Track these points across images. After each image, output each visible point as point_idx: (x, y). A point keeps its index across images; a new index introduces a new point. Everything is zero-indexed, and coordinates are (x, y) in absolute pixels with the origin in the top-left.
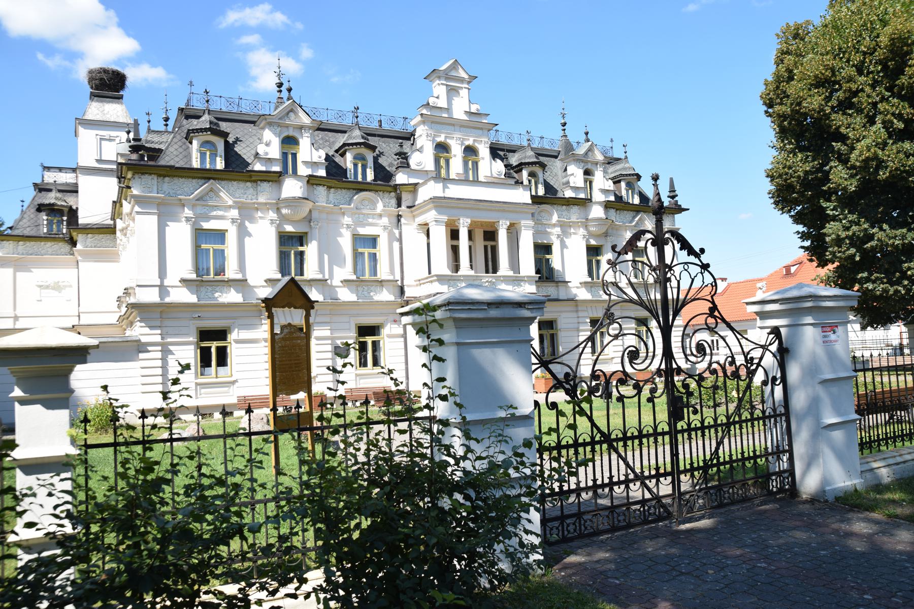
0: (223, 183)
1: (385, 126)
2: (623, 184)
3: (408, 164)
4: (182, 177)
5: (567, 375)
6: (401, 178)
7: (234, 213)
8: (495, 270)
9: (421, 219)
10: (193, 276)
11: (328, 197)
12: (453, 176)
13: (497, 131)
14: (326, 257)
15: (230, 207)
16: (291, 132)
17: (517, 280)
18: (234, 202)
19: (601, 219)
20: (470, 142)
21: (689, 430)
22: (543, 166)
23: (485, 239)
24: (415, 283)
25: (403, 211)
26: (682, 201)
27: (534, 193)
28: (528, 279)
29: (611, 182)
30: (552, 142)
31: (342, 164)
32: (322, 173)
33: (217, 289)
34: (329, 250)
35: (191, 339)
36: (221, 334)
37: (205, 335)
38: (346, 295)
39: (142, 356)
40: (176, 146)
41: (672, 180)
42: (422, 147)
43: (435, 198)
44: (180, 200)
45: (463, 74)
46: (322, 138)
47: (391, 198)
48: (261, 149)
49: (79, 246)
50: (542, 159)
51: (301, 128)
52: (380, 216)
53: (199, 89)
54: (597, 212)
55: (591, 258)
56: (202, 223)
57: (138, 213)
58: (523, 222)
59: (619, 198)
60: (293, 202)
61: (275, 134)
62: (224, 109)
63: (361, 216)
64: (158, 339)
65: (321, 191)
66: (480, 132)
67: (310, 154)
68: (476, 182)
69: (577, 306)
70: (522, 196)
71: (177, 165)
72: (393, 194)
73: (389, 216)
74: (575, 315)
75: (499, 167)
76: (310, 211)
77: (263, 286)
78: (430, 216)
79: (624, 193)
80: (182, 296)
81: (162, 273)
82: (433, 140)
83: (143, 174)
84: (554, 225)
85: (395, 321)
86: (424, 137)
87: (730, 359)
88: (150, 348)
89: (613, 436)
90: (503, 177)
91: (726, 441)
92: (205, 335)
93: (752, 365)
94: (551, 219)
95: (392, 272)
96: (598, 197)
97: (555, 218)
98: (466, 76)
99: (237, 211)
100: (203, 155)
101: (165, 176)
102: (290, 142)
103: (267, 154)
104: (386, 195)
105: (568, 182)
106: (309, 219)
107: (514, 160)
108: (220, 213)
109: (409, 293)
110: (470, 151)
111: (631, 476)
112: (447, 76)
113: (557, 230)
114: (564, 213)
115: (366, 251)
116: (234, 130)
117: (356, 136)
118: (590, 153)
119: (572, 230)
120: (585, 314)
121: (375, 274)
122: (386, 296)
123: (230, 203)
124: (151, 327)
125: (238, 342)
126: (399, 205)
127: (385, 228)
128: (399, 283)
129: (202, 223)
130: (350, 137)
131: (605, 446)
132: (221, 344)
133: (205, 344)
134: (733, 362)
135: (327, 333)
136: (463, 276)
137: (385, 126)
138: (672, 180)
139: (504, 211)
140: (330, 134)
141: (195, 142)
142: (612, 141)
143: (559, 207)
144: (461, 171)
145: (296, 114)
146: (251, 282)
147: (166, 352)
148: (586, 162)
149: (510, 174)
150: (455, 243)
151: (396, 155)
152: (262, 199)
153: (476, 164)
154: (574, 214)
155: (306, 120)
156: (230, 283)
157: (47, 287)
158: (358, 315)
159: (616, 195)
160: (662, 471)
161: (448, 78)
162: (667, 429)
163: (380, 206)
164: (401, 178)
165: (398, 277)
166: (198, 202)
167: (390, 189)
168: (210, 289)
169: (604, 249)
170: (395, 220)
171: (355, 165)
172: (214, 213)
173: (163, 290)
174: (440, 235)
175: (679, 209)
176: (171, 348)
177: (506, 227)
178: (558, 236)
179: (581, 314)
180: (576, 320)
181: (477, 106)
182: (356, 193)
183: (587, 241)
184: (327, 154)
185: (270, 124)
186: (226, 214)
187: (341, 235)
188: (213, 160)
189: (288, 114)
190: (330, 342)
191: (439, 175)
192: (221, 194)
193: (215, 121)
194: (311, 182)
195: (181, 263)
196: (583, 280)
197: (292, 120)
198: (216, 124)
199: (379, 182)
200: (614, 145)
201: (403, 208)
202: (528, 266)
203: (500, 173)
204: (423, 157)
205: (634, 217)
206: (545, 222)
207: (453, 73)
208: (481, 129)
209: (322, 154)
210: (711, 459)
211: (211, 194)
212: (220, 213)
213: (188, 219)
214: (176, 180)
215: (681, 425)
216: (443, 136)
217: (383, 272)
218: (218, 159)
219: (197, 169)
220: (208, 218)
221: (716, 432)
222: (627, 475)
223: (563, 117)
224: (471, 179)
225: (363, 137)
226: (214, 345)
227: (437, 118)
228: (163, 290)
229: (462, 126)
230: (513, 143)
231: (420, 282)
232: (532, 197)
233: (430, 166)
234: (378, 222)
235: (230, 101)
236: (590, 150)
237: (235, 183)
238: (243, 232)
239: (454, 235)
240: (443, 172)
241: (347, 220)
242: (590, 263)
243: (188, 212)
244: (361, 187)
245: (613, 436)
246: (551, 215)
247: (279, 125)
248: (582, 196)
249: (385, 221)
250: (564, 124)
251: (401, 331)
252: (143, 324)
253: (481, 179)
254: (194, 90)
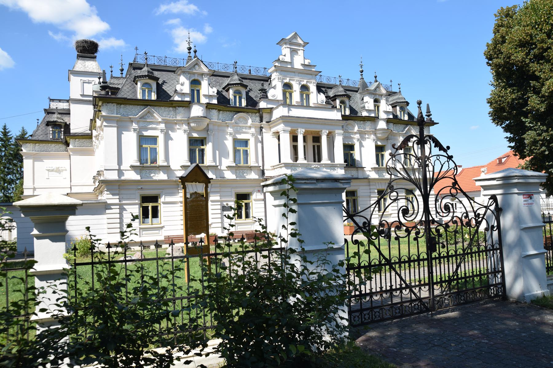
0: (156, 108)
1: (253, 73)
2: (398, 108)
3: (267, 97)
4: (131, 104)
5: (364, 223)
6: (262, 105)
7: (162, 126)
8: (320, 160)
9: (274, 130)
10: (138, 164)
11: (218, 116)
12: (294, 103)
13: (321, 76)
14: (217, 152)
15: (160, 122)
16: (196, 77)
17: (333, 167)
18: (162, 119)
19: (384, 129)
20: (304, 82)
21: (440, 258)
22: (349, 97)
23: (314, 141)
24: (271, 168)
25: (264, 124)
26: (434, 118)
27: (343, 114)
28: (340, 166)
29: (390, 107)
30: (354, 82)
31: (227, 96)
32: (215, 101)
33: (152, 171)
34: (219, 148)
35: (137, 202)
36: (155, 199)
37: (145, 199)
38: (229, 175)
39: (108, 211)
40: (128, 86)
41: (428, 106)
42: (275, 86)
43: (283, 116)
44: (130, 118)
45: (300, 42)
46: (215, 81)
47: (257, 117)
48: (178, 88)
49: (71, 146)
50: (348, 93)
51: (202, 74)
52: (250, 127)
53: (141, 52)
54: (382, 125)
55: (378, 153)
56: (143, 132)
57: (105, 126)
58: (337, 131)
59: (395, 117)
60: (197, 119)
61: (186, 78)
62: (156, 64)
63: (238, 128)
64: (117, 201)
65: (214, 112)
66: (310, 76)
67: (207, 90)
68: (308, 107)
69: (369, 182)
70: (336, 115)
71: (128, 98)
72: (258, 114)
73: (255, 128)
74: (368, 187)
75: (322, 97)
76: (208, 125)
77: (180, 170)
78: (280, 127)
79: (398, 113)
80: (132, 175)
81: (120, 162)
82: (282, 82)
83: (108, 103)
84: (356, 133)
85: (259, 191)
86: (277, 80)
87: (465, 214)
88: (112, 207)
89: (393, 261)
90: (324, 103)
91: (462, 265)
92: (145, 199)
93: (479, 218)
94: (354, 129)
95: (257, 161)
96: (383, 116)
97: (356, 129)
98: (302, 43)
99: (164, 125)
100: (144, 91)
101: (121, 104)
102: (195, 83)
103: (182, 90)
104: (254, 115)
105: (364, 107)
106: (207, 129)
107: (331, 93)
108: (154, 126)
109: (267, 174)
110: (304, 88)
111: (404, 286)
112: (290, 42)
113: (358, 136)
114: (362, 126)
115: (242, 149)
116: (162, 76)
117: (236, 79)
118: (378, 89)
119: (367, 136)
120: (375, 187)
121: (247, 163)
122: (253, 176)
123: (160, 120)
124: (113, 195)
125: (164, 203)
126: (261, 121)
127: (253, 135)
128: (261, 168)
129: (143, 132)
130: (231, 80)
131: (387, 267)
132: (154, 204)
133: (145, 205)
134: (467, 216)
135: (218, 198)
136: (300, 164)
137: (253, 73)
138: (428, 106)
139: (325, 124)
140: (220, 78)
141: (139, 84)
142: (391, 81)
143: (359, 122)
144: (299, 100)
145: (199, 66)
146: (173, 167)
147: (122, 209)
148: (375, 95)
149: (328, 102)
150: (295, 144)
151: (259, 90)
152: (179, 118)
153: (308, 96)
154: (368, 126)
155: (205, 70)
156: (160, 168)
157: (52, 171)
158: (237, 187)
159: (393, 115)
160: (422, 283)
161: (291, 44)
162: (426, 257)
163: (250, 122)
164: (262, 105)
165: (261, 164)
166: (141, 120)
167: (255, 111)
168: (148, 171)
169: (386, 148)
170: (259, 130)
171: (235, 97)
172: (151, 126)
173: (120, 172)
174: (286, 139)
175: (433, 123)
176: (125, 207)
177: (326, 134)
178: (358, 140)
179: (372, 187)
180: (369, 191)
181: (309, 61)
182: (236, 114)
183: (376, 142)
184: (218, 90)
185: (184, 73)
186: (157, 127)
187: (226, 139)
188: (150, 95)
189: (194, 66)
190: (219, 203)
191: (286, 102)
192: (155, 115)
193: (151, 71)
194: (208, 107)
195: (131, 156)
196: (373, 166)
197: (197, 70)
198: (152, 73)
199: (249, 107)
200: (393, 84)
201: (264, 122)
202: (339, 158)
203: (322, 101)
204: (276, 92)
205: (405, 128)
206: (350, 131)
207: (294, 41)
208: (311, 74)
209: (215, 90)
210: (453, 276)
211: (149, 114)
212: (154, 126)
213: (135, 130)
214: (128, 107)
215: (434, 254)
216: (288, 79)
217: (252, 162)
218: (153, 94)
219: (140, 100)
220: (147, 129)
221: (457, 259)
222: (401, 285)
223: (361, 67)
224: (305, 105)
225: (239, 80)
226: (150, 205)
227: (285, 69)
228: (120, 172)
229: (299, 73)
230: (331, 83)
231: (274, 168)
232: (342, 116)
233: (280, 97)
234: (249, 131)
235: (159, 59)
236: (378, 87)
237: (163, 108)
238: (168, 138)
239: (295, 139)
240: (288, 101)
241: (230, 130)
242: (377, 156)
243: (135, 126)
244: (238, 110)
245: (393, 261)
246: (354, 127)
247: (189, 73)
248: (373, 115)
249: (253, 130)
250: (362, 72)
251: (262, 197)
252: (108, 193)
253: (311, 105)
254: (138, 52)
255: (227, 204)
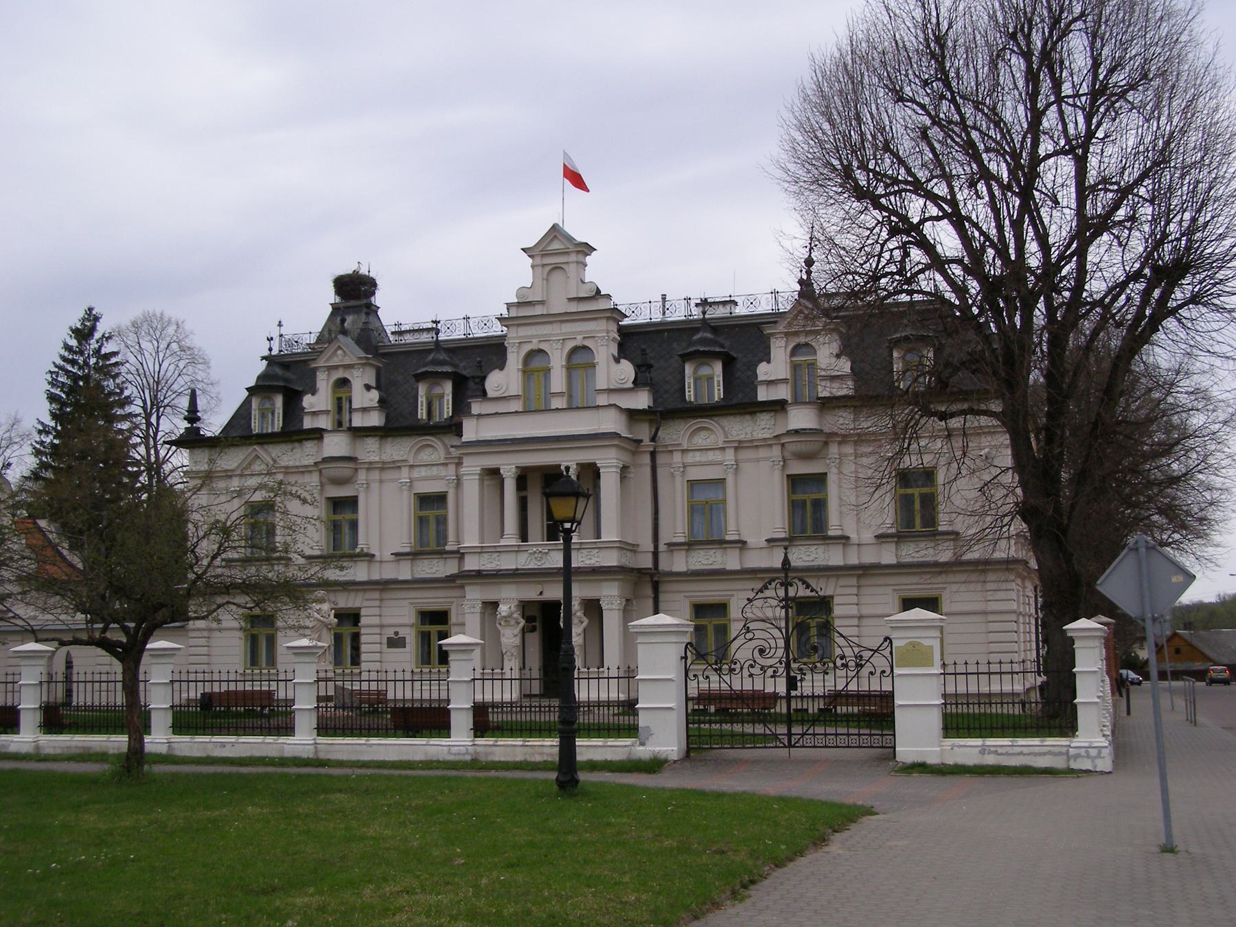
3: (484, 393)
16: (340, 374)
28: (609, 546)
65: (372, 443)
90: (631, 386)
100: (263, 416)
103: (312, 405)
110: (579, 359)
207: (556, 245)
255: (396, 633)
